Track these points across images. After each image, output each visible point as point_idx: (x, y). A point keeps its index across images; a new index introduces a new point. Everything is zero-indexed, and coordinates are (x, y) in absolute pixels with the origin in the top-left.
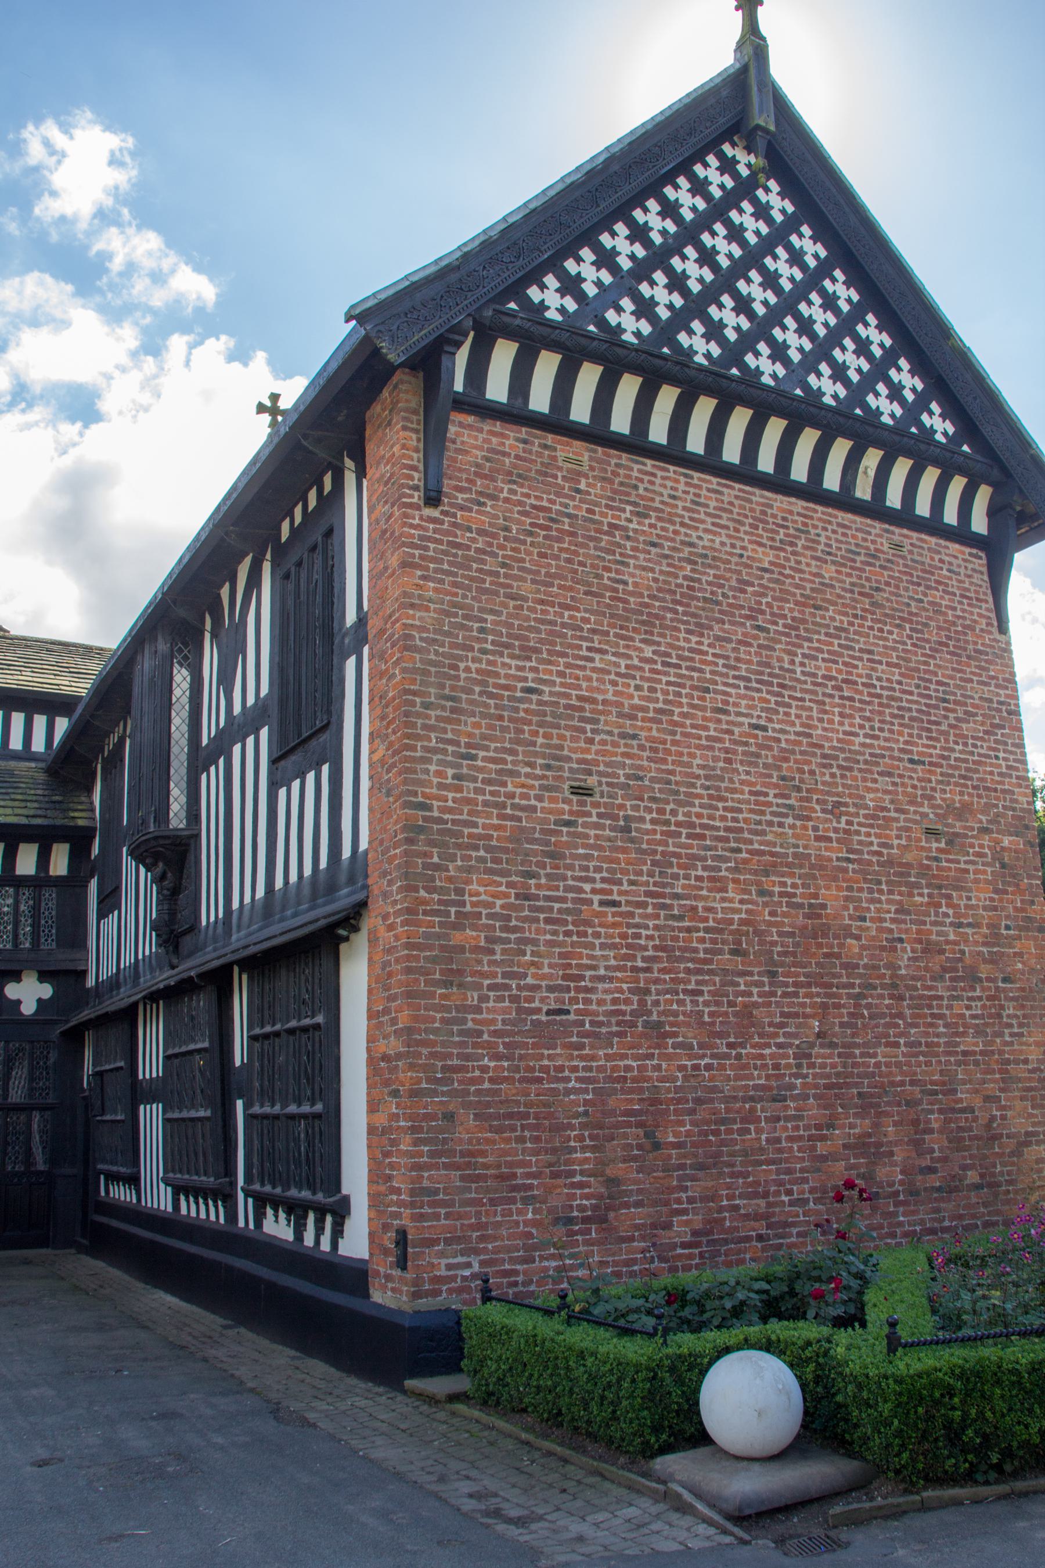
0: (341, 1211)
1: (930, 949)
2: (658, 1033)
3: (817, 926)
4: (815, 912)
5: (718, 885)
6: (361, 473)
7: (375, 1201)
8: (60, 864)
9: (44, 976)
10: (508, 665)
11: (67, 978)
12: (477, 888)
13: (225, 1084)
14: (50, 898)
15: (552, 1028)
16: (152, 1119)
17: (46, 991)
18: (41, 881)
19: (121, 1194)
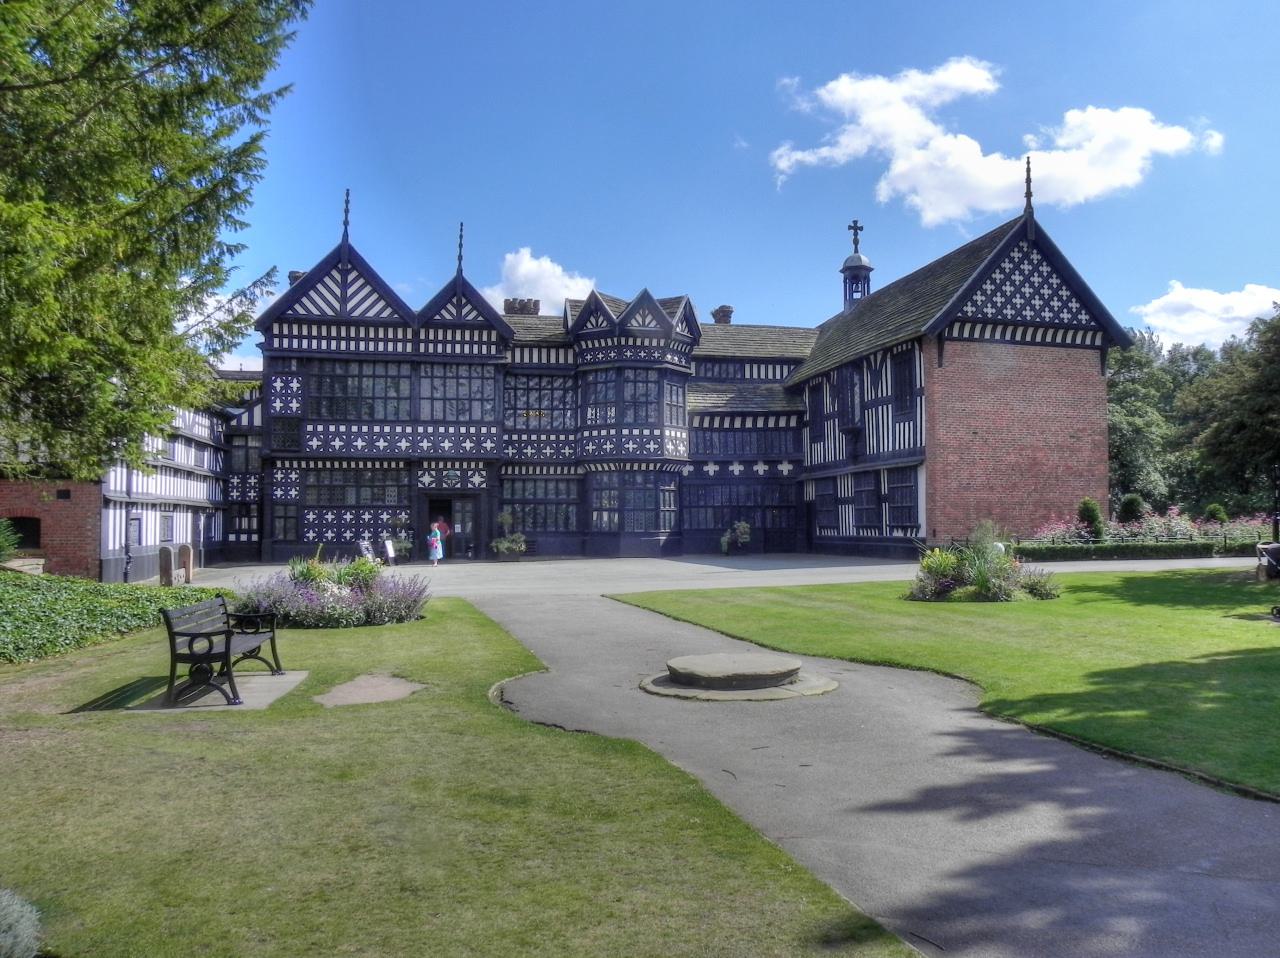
0: (918, 528)
1: (1069, 468)
2: (992, 488)
3: (1035, 462)
4: (1035, 459)
5: (1009, 454)
6: (921, 350)
7: (928, 524)
8: (793, 423)
9: (790, 462)
10: (958, 405)
11: (797, 463)
12: (951, 458)
13: (880, 500)
14: (790, 434)
15: (967, 488)
16: (885, 507)
17: (791, 467)
18: (788, 428)
19: (829, 533)
